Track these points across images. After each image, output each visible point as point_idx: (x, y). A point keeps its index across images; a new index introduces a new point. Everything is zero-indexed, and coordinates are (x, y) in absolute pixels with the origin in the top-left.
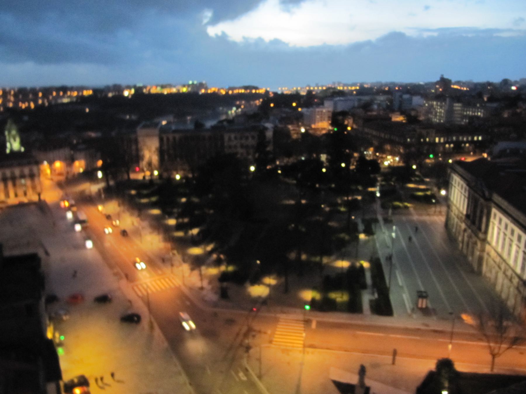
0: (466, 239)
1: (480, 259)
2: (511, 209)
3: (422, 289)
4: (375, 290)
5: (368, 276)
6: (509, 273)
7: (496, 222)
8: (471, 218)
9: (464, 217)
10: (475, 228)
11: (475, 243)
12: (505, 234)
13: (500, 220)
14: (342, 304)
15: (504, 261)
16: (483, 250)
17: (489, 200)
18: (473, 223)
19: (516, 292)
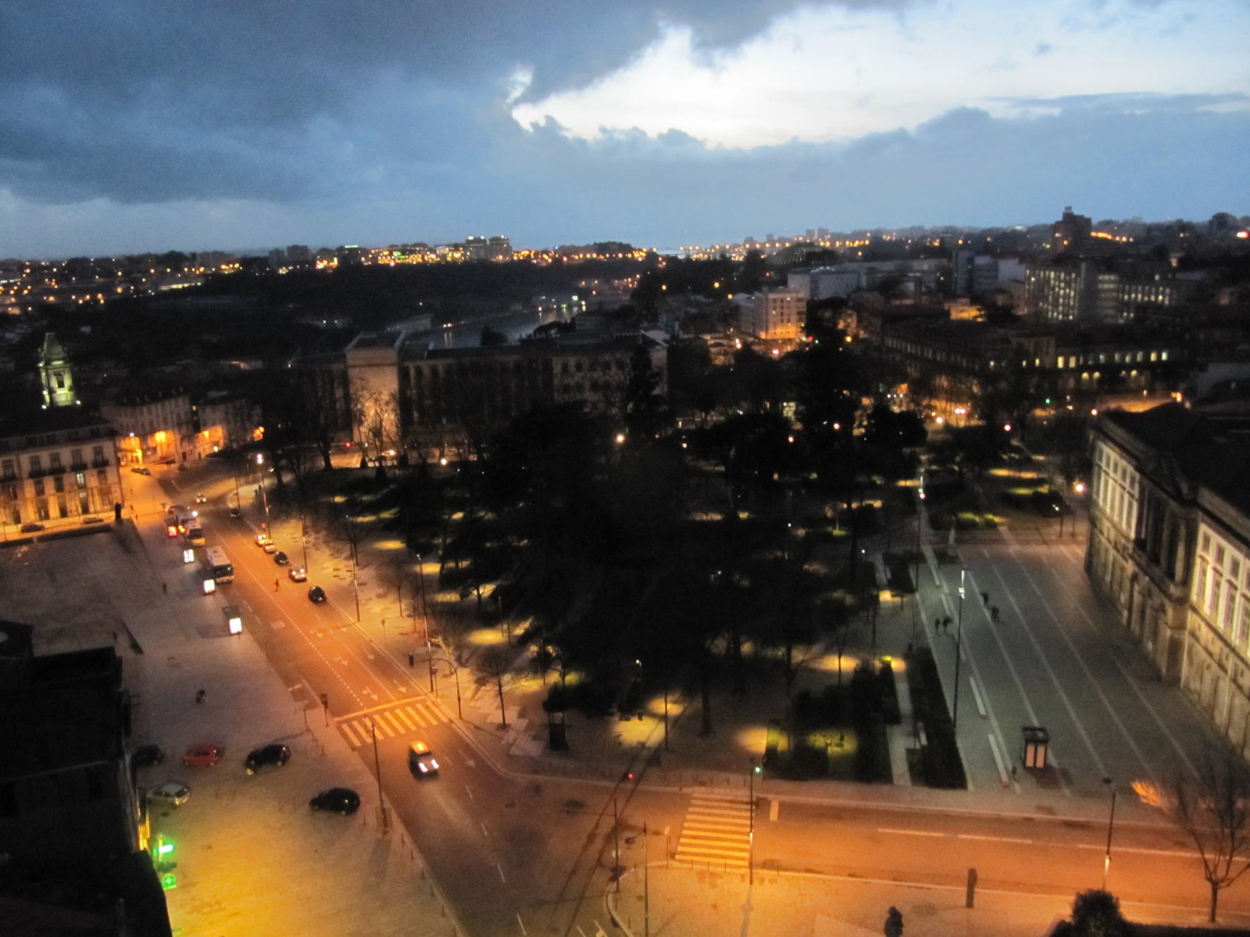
0: (1137, 598)
1: (1175, 648)
3: (1036, 723)
4: (920, 724)
5: (902, 689)
7: (1211, 557)
8: (1148, 548)
9: (1130, 546)
11: (1162, 609)
12: (1232, 586)
14: (843, 758)
15: (1233, 650)
16: (1180, 626)
17: (1192, 503)
18: (1155, 560)
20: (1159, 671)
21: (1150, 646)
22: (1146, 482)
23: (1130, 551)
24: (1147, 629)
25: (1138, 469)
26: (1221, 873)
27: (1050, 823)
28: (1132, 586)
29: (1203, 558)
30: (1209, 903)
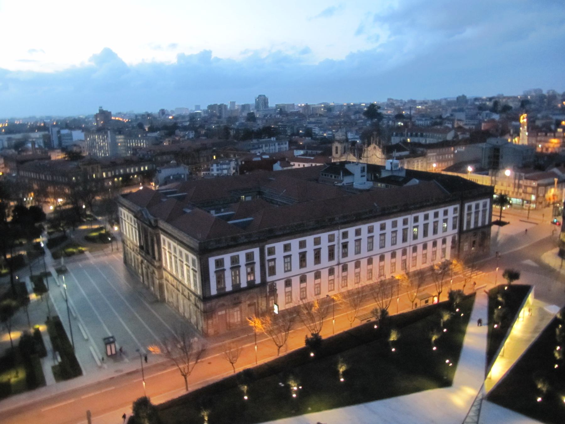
0: (144, 270)
1: (161, 286)
2: (175, 232)
3: (110, 335)
4: (57, 353)
5: (47, 340)
6: (186, 293)
7: (166, 248)
8: (145, 248)
9: (138, 249)
10: (149, 257)
11: (153, 272)
12: (176, 257)
13: (169, 245)
14: (19, 382)
15: (180, 282)
16: (161, 277)
17: (156, 227)
18: (147, 253)
19: (195, 308)
20: (157, 298)
21: (152, 289)
22: (139, 221)
23: (138, 251)
24: (150, 283)
25: (135, 216)
26: (186, 371)
27: (122, 376)
28: (142, 265)
29: (164, 248)
30: (185, 384)
